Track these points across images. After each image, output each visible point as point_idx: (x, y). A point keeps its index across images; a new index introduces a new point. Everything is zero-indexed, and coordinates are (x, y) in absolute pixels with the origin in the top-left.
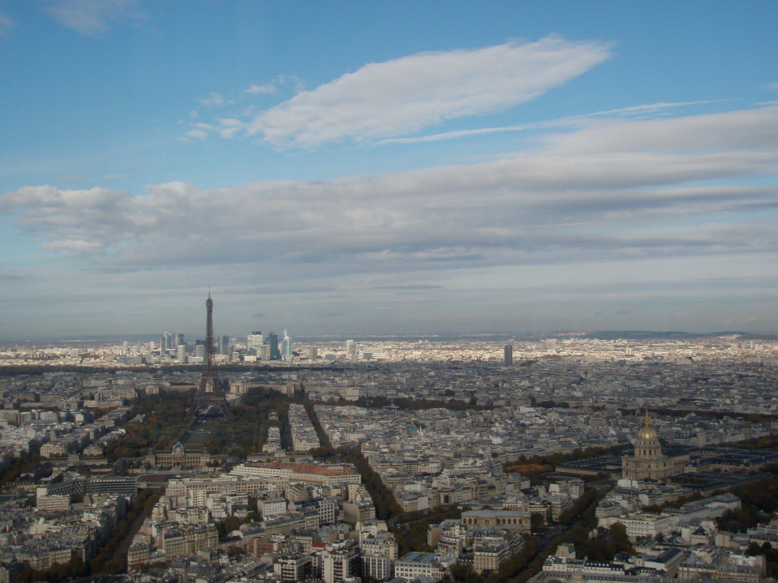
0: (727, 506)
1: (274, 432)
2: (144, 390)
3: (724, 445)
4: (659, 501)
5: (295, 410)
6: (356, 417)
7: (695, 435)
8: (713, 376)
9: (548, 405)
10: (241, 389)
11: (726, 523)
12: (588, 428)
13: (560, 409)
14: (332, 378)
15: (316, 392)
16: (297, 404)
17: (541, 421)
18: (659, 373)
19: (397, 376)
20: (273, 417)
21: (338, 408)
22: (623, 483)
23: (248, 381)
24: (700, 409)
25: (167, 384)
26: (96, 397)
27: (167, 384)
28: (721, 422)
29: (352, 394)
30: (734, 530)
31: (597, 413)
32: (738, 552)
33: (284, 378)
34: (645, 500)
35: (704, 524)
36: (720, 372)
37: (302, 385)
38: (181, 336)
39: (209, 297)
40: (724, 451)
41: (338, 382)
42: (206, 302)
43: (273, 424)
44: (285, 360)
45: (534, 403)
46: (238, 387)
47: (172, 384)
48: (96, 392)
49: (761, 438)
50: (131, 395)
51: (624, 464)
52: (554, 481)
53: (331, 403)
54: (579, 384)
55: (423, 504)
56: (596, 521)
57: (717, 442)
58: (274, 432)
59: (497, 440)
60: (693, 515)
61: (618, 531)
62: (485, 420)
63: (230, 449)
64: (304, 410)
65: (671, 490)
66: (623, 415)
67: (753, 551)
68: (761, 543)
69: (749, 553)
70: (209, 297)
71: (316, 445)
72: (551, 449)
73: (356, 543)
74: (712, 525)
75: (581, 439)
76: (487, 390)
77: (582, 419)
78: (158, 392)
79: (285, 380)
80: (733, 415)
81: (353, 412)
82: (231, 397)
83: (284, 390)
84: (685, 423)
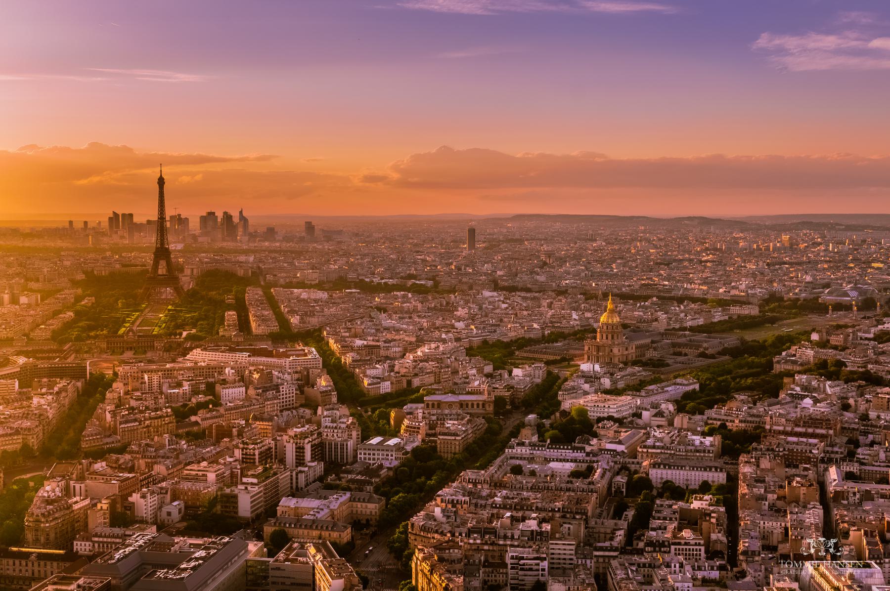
2: (93, 271)
3: (685, 329)
4: (621, 385)
5: (253, 294)
6: (316, 301)
7: (656, 320)
8: (675, 261)
9: (512, 289)
10: (195, 271)
12: (550, 313)
13: (523, 294)
15: (275, 276)
17: (504, 306)
18: (622, 258)
22: (585, 367)
24: (662, 294)
25: (118, 266)
28: (682, 307)
29: (313, 276)
30: (693, 412)
31: (560, 298)
32: (695, 432)
34: (607, 382)
36: (680, 257)
37: (259, 268)
40: (685, 336)
43: (229, 307)
45: (496, 286)
46: (192, 269)
47: (124, 266)
49: (720, 321)
50: (80, 277)
51: (586, 348)
53: (290, 285)
54: (541, 268)
55: (386, 387)
56: (559, 403)
57: (677, 326)
59: (460, 325)
60: (653, 399)
62: (448, 303)
65: (633, 374)
66: (587, 299)
67: (710, 433)
69: (704, 434)
73: (319, 425)
74: (671, 407)
75: (544, 323)
76: (449, 274)
77: (545, 303)
80: (694, 300)
83: (240, 273)
84: (646, 308)
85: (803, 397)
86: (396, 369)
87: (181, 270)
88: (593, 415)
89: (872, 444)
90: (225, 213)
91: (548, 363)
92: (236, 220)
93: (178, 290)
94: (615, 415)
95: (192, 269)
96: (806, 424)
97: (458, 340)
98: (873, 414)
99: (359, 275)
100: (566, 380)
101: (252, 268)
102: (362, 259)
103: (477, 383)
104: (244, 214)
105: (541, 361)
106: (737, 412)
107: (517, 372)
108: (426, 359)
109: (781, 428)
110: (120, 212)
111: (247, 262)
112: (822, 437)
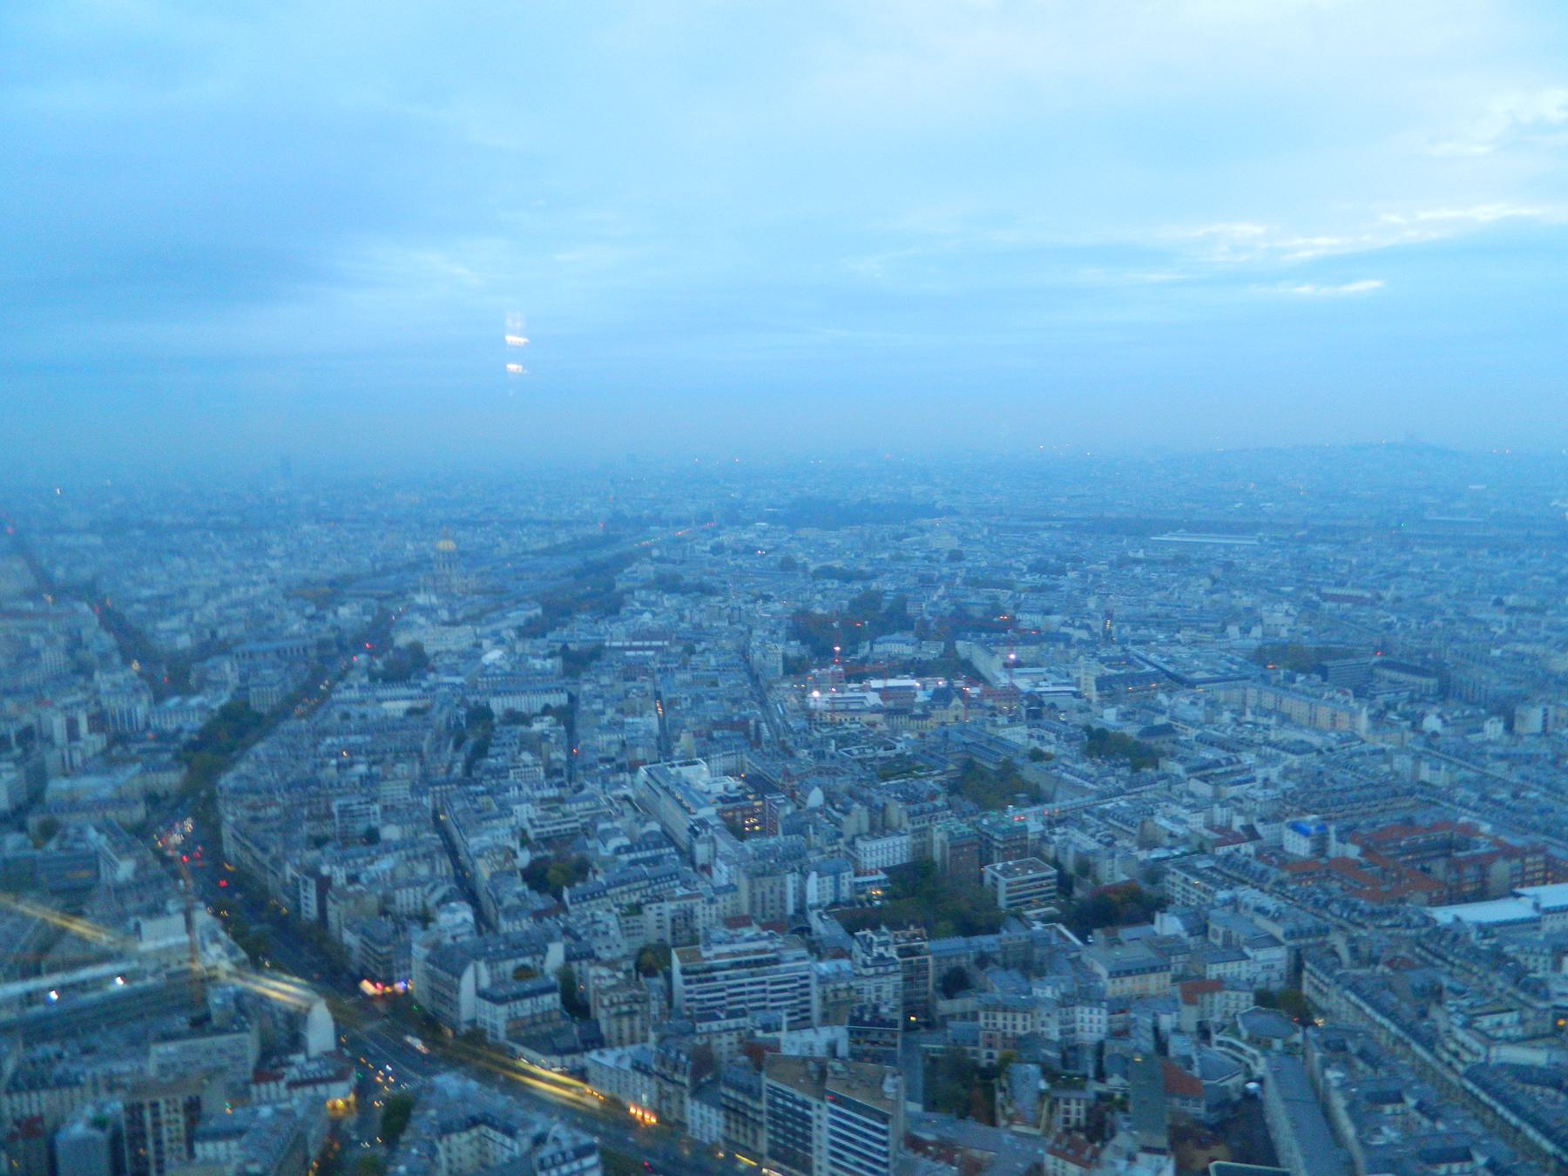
0: (531, 613)
4: (459, 616)
11: (530, 630)
22: (421, 599)
30: (534, 636)
32: (536, 656)
34: (444, 615)
35: (504, 634)
52: (342, 604)
55: (184, 642)
56: (392, 640)
60: (495, 626)
61: (416, 649)
65: (472, 603)
67: (552, 655)
68: (558, 646)
69: (545, 658)
72: (339, 570)
74: (512, 634)
85: (641, 613)
86: (197, 618)
88: (429, 649)
89: (703, 652)
91: (380, 599)
94: (454, 648)
96: (643, 638)
97: (272, 581)
98: (706, 624)
100: (399, 615)
103: (296, 627)
105: (372, 596)
106: (579, 632)
107: (344, 611)
108: (234, 605)
109: (619, 644)
112: (657, 649)
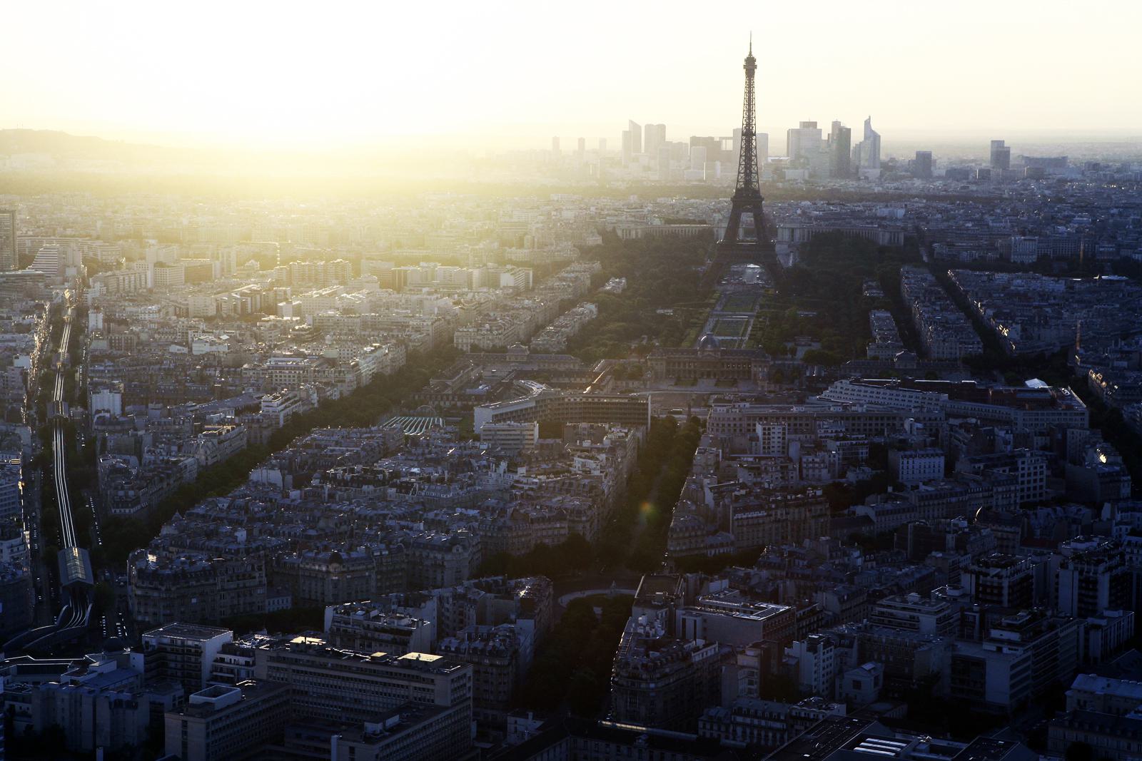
1: (880, 318)
6: (1043, 296)
10: (797, 234)
14: (977, 216)
15: (951, 245)
16: (916, 267)
19: (1113, 215)
20: (871, 291)
21: (1001, 277)
23: (810, 218)
26: (527, 244)
27: (657, 222)
33: (879, 213)
37: (917, 229)
38: (662, 128)
39: (751, 52)
41: (991, 224)
42: (744, 63)
43: (873, 304)
44: (866, 178)
48: (526, 234)
50: (595, 240)
58: (880, 318)
63: (801, 353)
64: (933, 279)
70: (751, 52)
71: (976, 348)
78: (639, 236)
79: (884, 218)
81: (1035, 285)
82: (778, 248)
83: (884, 238)
87: (774, 232)
90: (836, 125)
92: (857, 137)
93: (771, 267)
95: (793, 230)
99: (1119, 246)
101: (904, 229)
102: (1120, 214)
104: (874, 127)
110: (642, 122)
111: (892, 218)
